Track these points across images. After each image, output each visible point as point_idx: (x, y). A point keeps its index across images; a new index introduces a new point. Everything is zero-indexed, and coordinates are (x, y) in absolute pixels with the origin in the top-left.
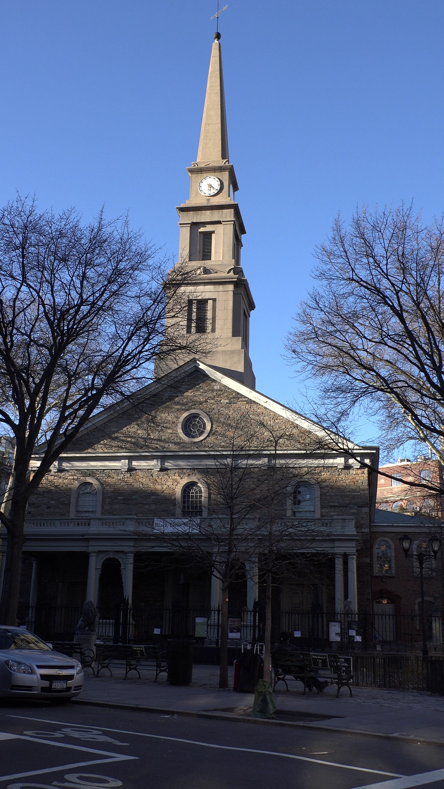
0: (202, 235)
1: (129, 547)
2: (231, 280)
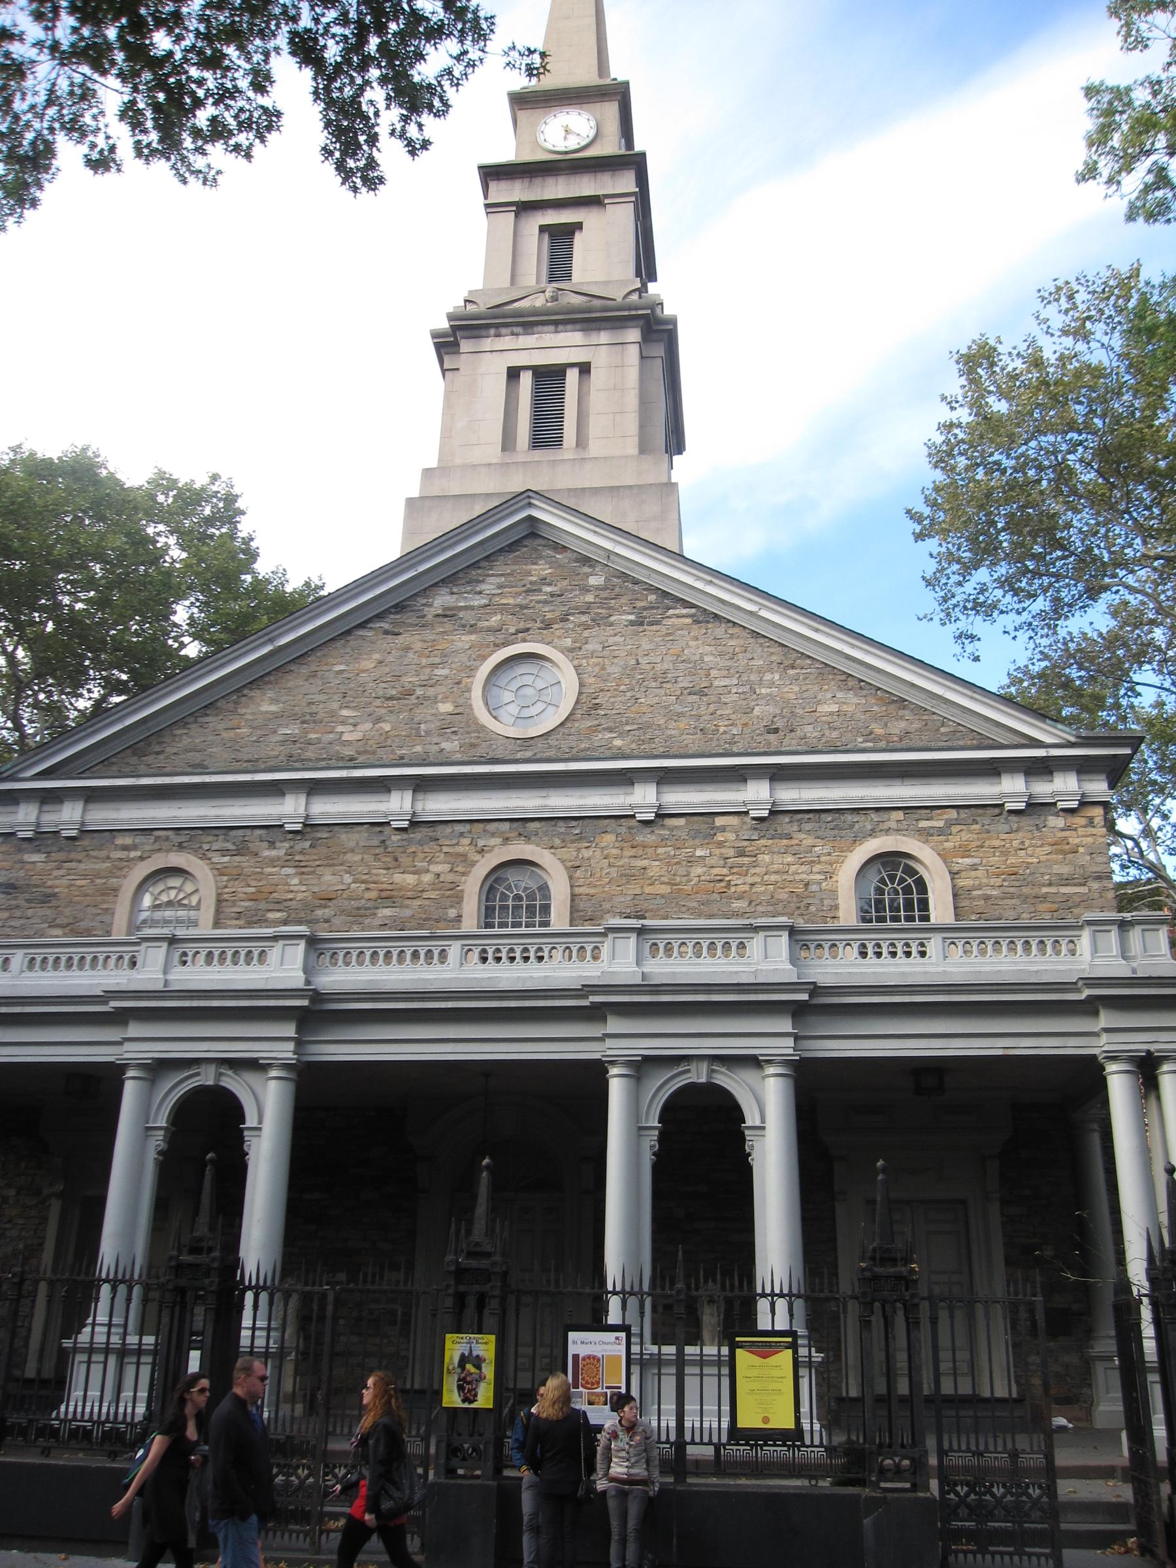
0: (546, 237)
1: (277, 1044)
2: (633, 313)
